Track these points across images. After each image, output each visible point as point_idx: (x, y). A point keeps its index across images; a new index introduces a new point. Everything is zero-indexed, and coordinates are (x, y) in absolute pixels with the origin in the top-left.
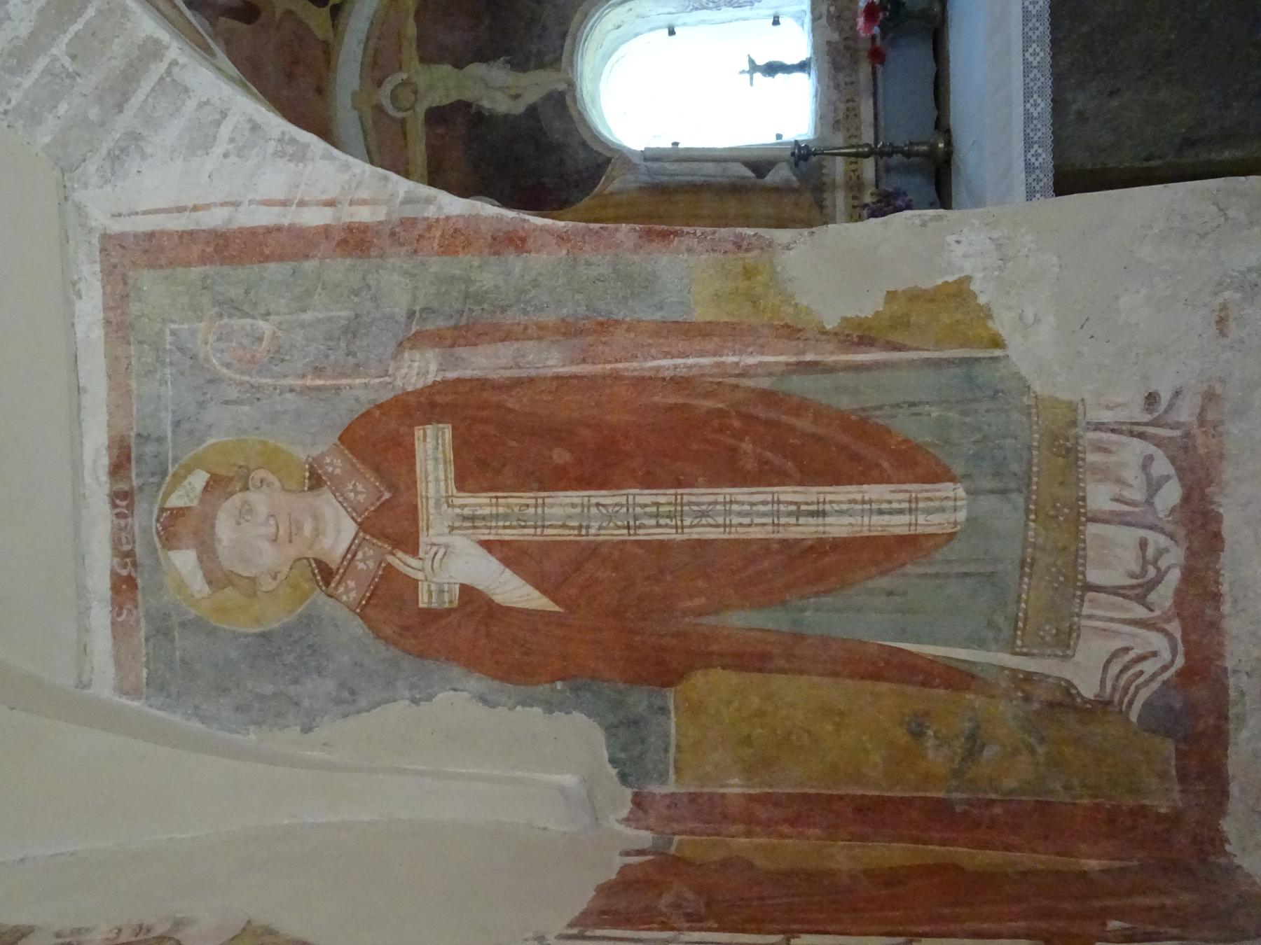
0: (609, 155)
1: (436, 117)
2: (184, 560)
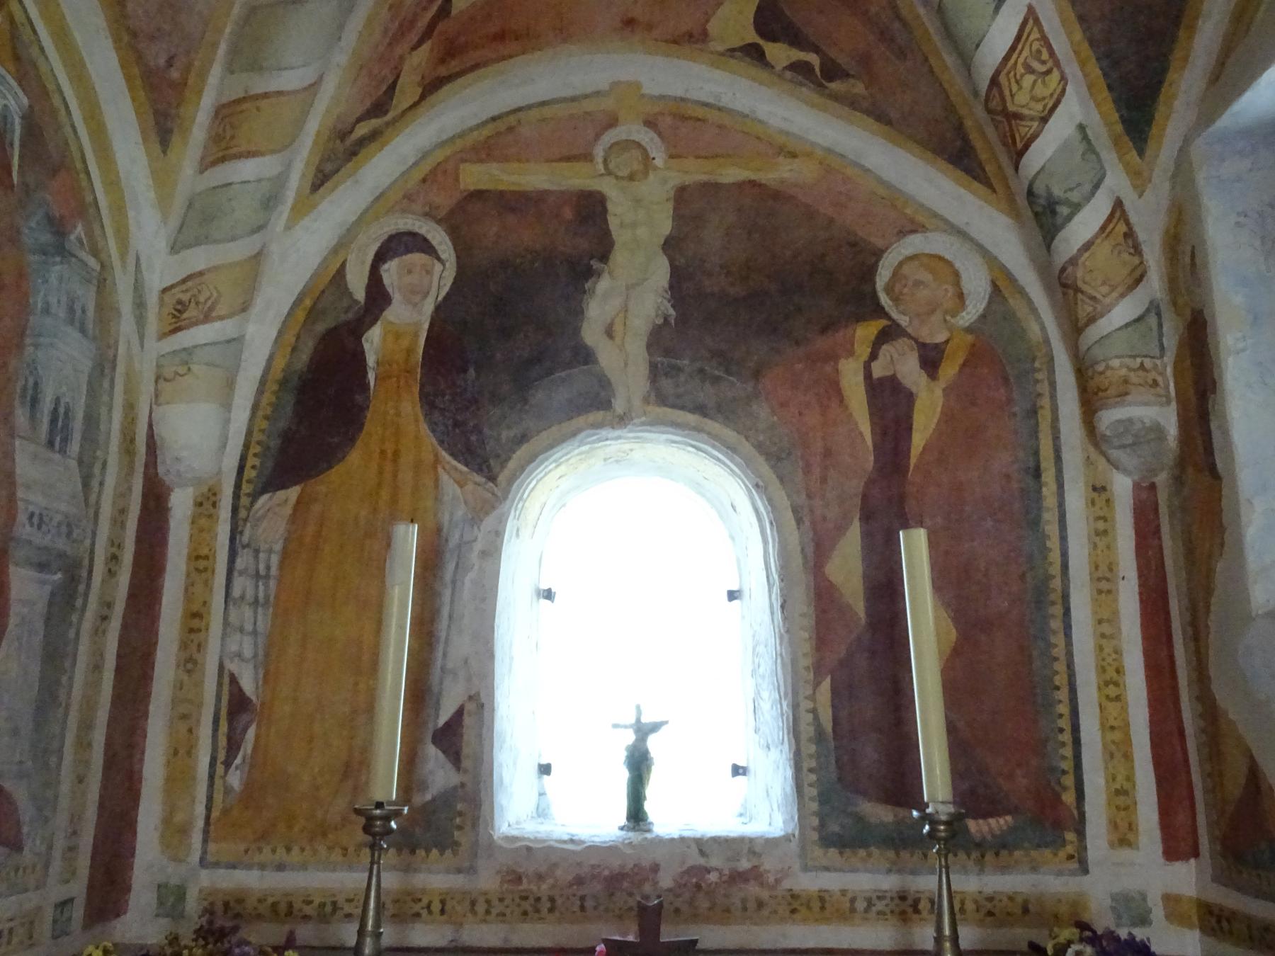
0: (502, 478)
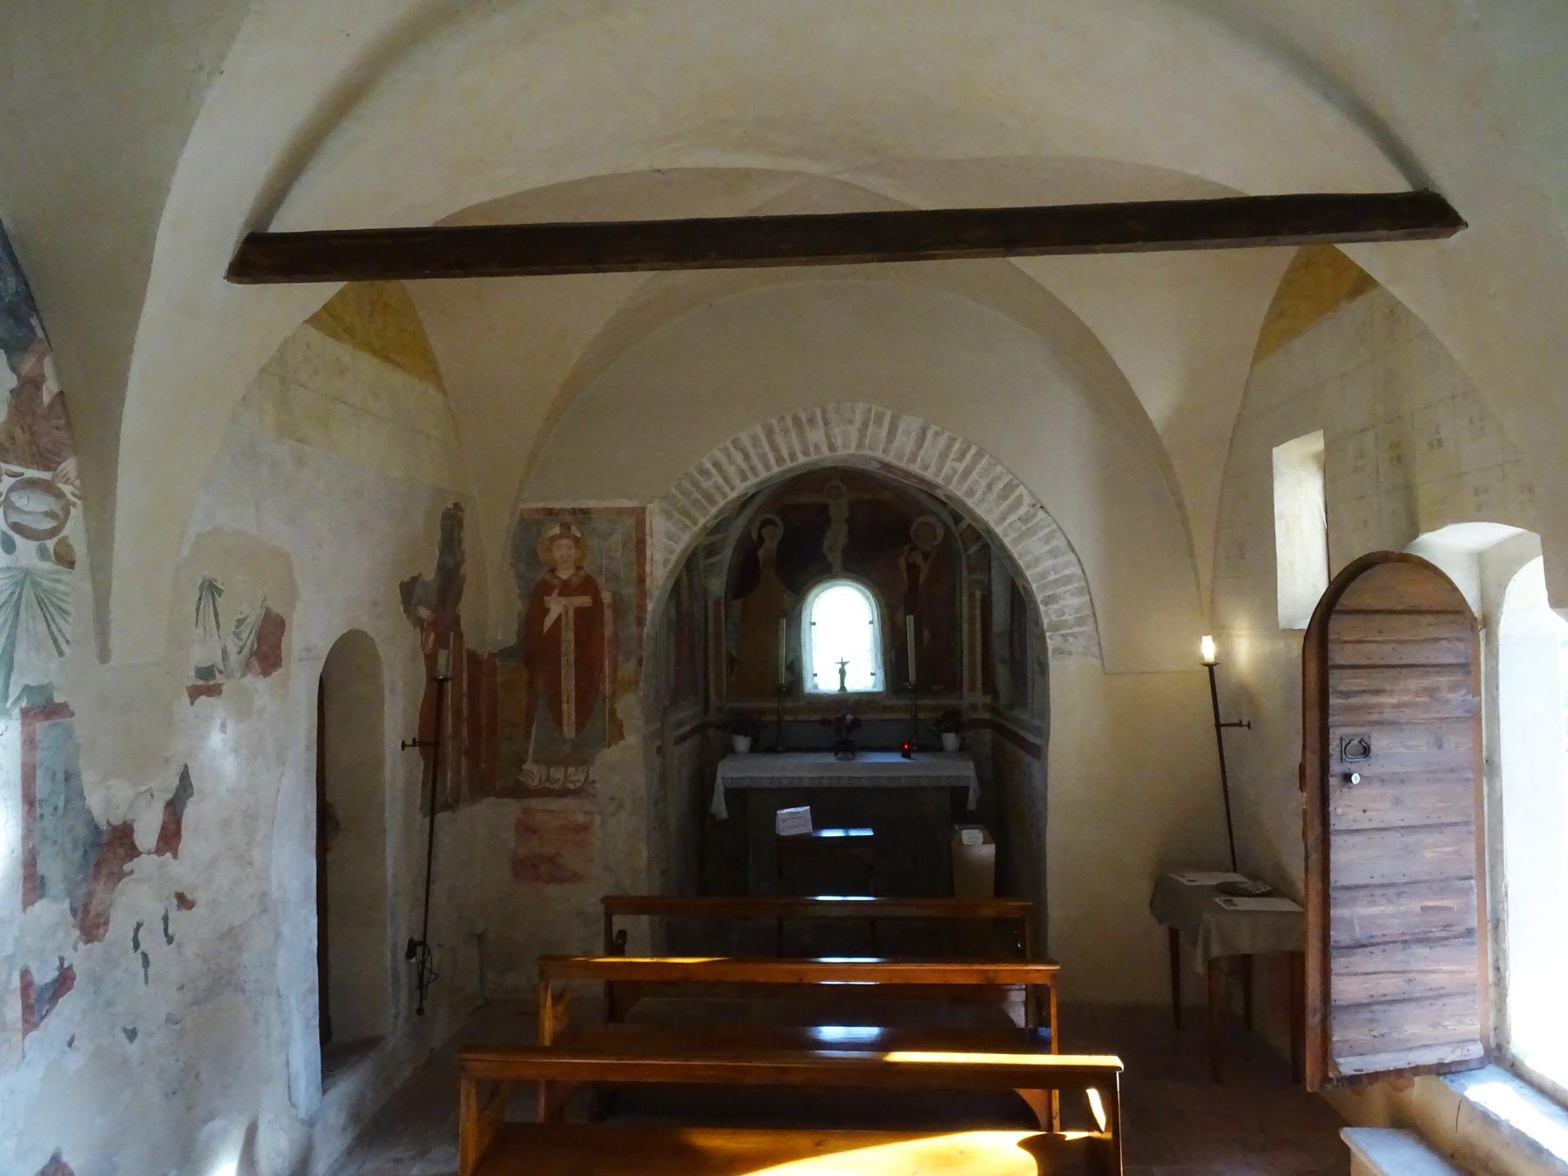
1: (823, 510)
2: (557, 530)
